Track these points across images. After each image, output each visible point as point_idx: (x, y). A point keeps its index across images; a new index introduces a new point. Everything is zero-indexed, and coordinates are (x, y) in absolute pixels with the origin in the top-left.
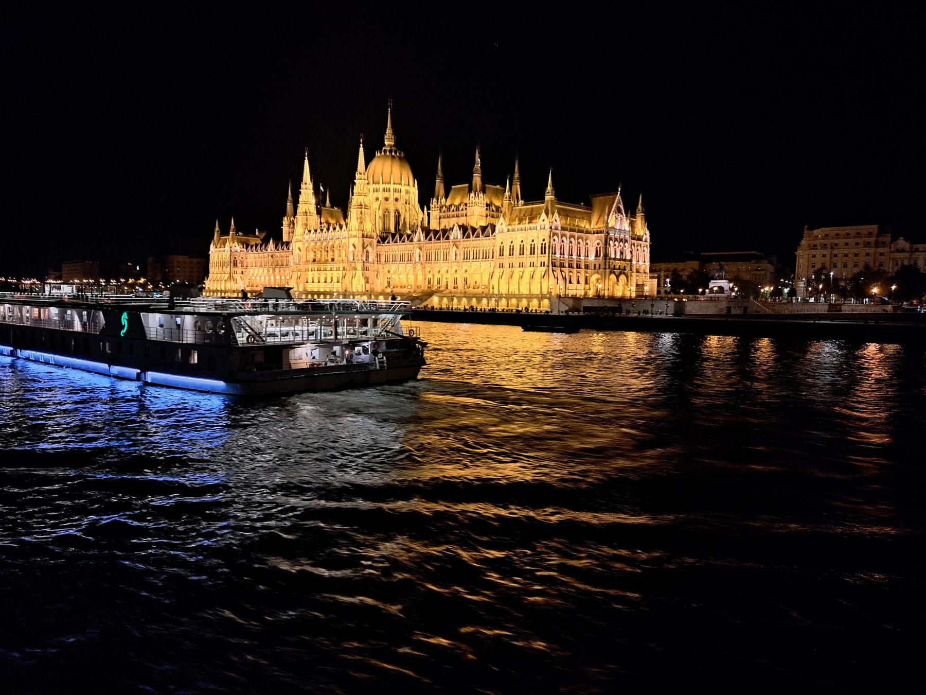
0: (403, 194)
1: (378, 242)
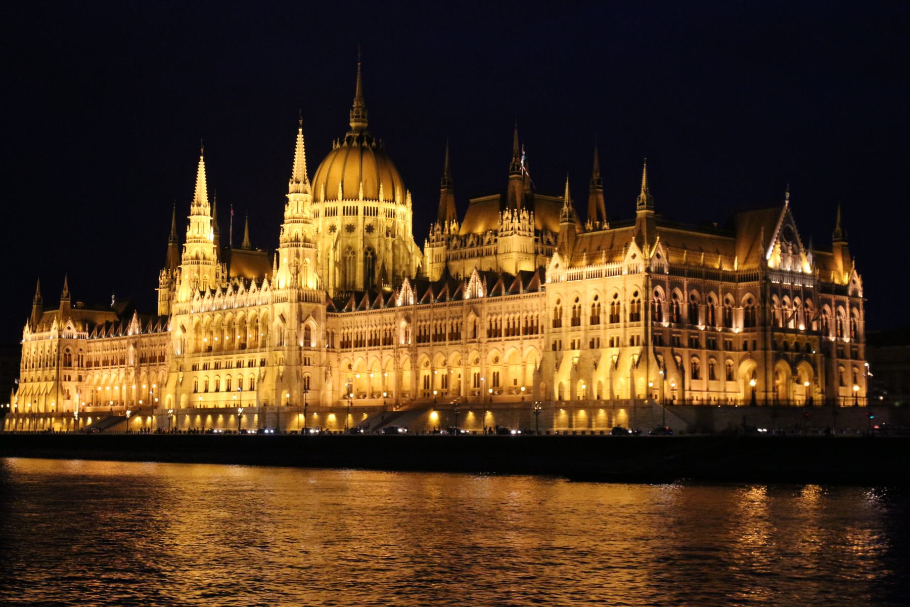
1: (329, 309)
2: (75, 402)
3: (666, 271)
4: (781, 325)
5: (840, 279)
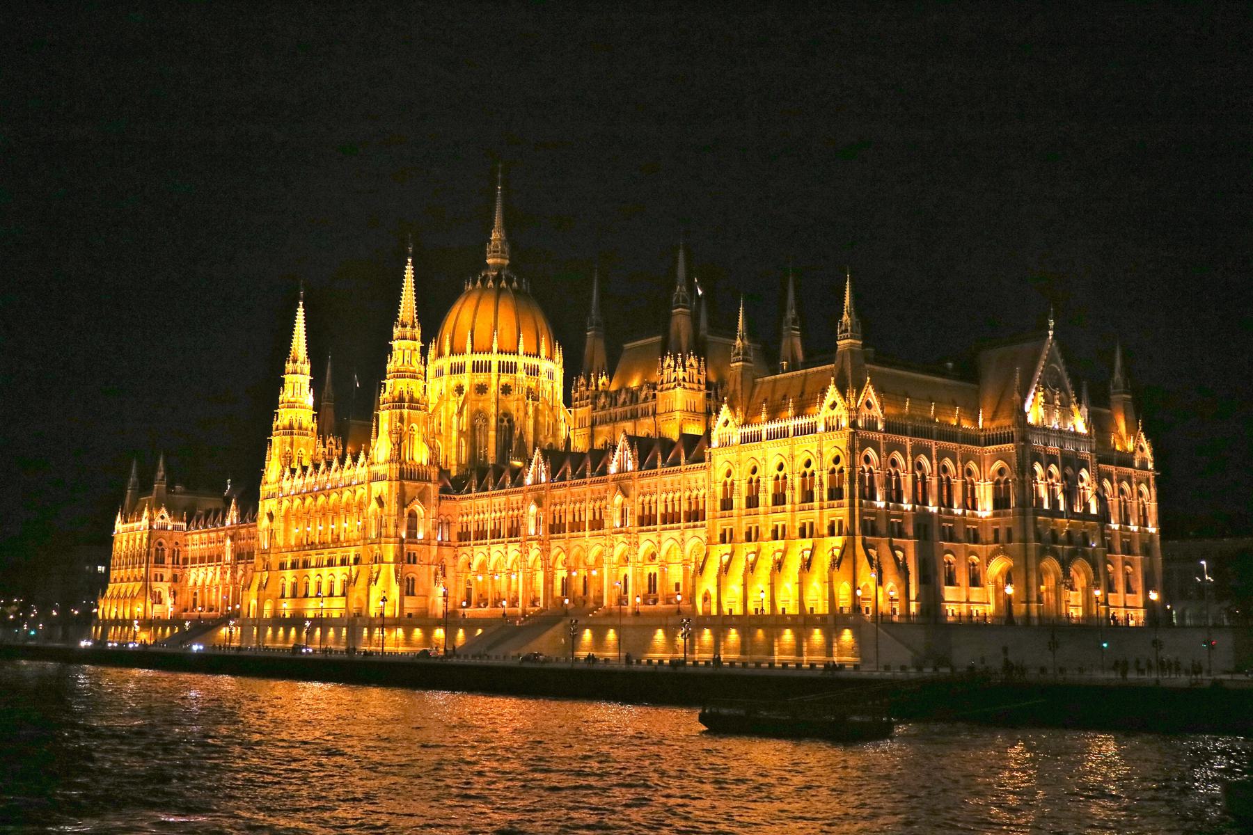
0: (521, 375)
1: (444, 490)
2: (167, 608)
3: (880, 426)
4: (1046, 506)
5: (1121, 445)
